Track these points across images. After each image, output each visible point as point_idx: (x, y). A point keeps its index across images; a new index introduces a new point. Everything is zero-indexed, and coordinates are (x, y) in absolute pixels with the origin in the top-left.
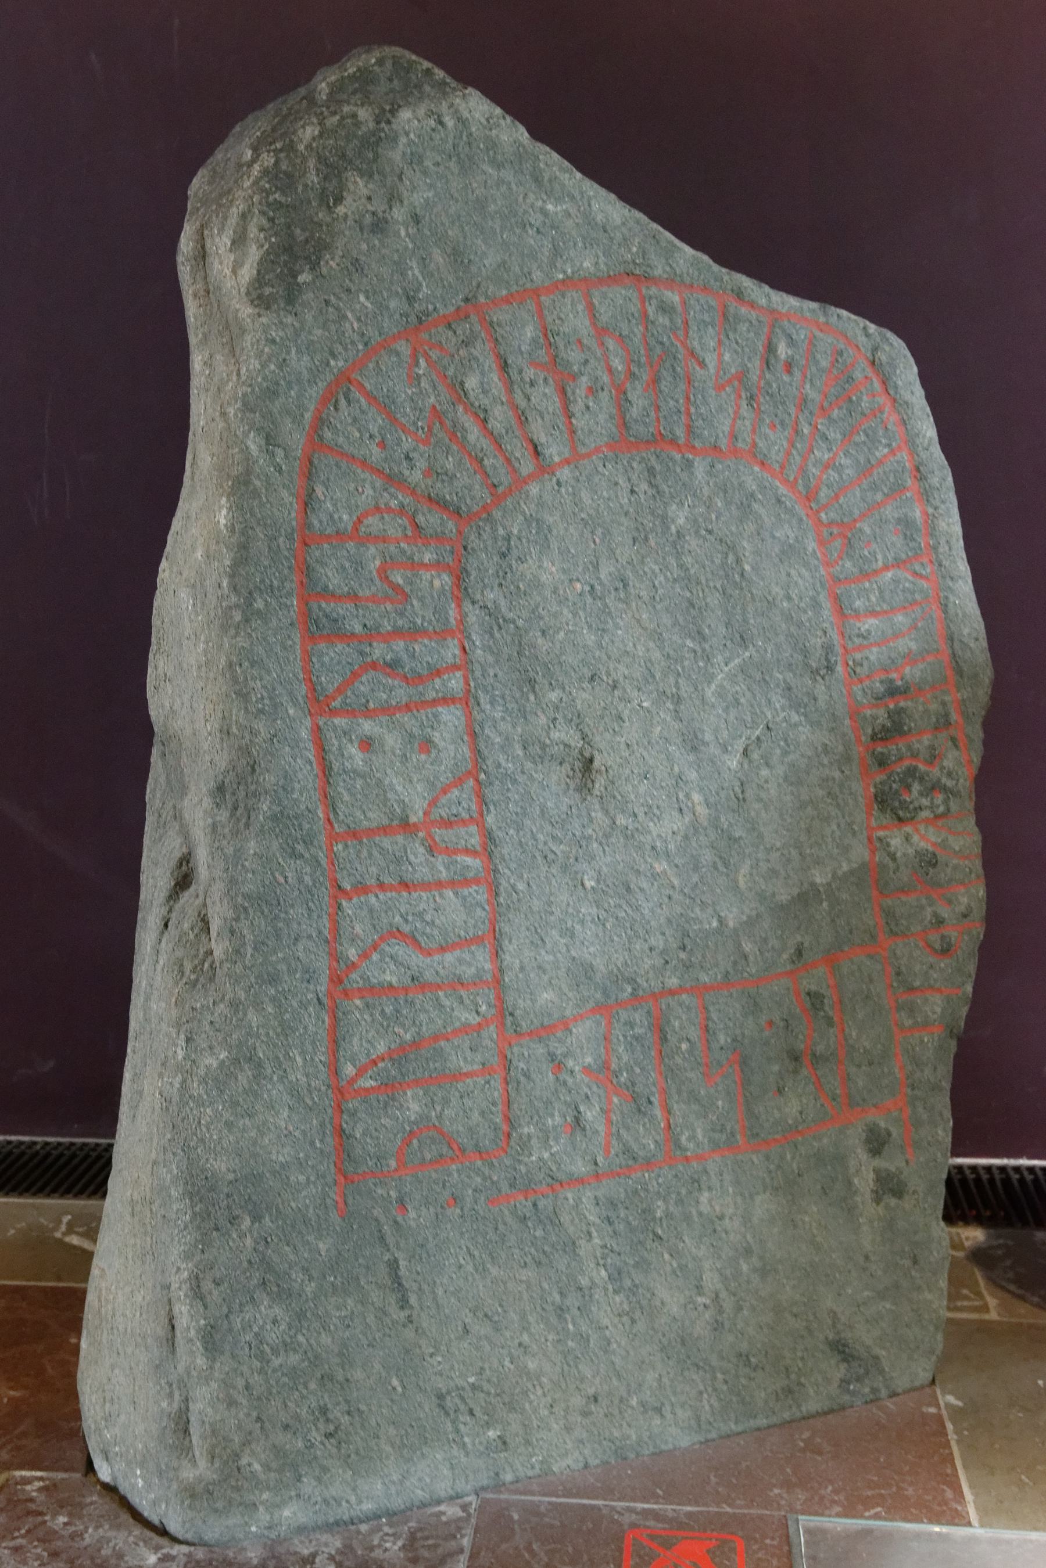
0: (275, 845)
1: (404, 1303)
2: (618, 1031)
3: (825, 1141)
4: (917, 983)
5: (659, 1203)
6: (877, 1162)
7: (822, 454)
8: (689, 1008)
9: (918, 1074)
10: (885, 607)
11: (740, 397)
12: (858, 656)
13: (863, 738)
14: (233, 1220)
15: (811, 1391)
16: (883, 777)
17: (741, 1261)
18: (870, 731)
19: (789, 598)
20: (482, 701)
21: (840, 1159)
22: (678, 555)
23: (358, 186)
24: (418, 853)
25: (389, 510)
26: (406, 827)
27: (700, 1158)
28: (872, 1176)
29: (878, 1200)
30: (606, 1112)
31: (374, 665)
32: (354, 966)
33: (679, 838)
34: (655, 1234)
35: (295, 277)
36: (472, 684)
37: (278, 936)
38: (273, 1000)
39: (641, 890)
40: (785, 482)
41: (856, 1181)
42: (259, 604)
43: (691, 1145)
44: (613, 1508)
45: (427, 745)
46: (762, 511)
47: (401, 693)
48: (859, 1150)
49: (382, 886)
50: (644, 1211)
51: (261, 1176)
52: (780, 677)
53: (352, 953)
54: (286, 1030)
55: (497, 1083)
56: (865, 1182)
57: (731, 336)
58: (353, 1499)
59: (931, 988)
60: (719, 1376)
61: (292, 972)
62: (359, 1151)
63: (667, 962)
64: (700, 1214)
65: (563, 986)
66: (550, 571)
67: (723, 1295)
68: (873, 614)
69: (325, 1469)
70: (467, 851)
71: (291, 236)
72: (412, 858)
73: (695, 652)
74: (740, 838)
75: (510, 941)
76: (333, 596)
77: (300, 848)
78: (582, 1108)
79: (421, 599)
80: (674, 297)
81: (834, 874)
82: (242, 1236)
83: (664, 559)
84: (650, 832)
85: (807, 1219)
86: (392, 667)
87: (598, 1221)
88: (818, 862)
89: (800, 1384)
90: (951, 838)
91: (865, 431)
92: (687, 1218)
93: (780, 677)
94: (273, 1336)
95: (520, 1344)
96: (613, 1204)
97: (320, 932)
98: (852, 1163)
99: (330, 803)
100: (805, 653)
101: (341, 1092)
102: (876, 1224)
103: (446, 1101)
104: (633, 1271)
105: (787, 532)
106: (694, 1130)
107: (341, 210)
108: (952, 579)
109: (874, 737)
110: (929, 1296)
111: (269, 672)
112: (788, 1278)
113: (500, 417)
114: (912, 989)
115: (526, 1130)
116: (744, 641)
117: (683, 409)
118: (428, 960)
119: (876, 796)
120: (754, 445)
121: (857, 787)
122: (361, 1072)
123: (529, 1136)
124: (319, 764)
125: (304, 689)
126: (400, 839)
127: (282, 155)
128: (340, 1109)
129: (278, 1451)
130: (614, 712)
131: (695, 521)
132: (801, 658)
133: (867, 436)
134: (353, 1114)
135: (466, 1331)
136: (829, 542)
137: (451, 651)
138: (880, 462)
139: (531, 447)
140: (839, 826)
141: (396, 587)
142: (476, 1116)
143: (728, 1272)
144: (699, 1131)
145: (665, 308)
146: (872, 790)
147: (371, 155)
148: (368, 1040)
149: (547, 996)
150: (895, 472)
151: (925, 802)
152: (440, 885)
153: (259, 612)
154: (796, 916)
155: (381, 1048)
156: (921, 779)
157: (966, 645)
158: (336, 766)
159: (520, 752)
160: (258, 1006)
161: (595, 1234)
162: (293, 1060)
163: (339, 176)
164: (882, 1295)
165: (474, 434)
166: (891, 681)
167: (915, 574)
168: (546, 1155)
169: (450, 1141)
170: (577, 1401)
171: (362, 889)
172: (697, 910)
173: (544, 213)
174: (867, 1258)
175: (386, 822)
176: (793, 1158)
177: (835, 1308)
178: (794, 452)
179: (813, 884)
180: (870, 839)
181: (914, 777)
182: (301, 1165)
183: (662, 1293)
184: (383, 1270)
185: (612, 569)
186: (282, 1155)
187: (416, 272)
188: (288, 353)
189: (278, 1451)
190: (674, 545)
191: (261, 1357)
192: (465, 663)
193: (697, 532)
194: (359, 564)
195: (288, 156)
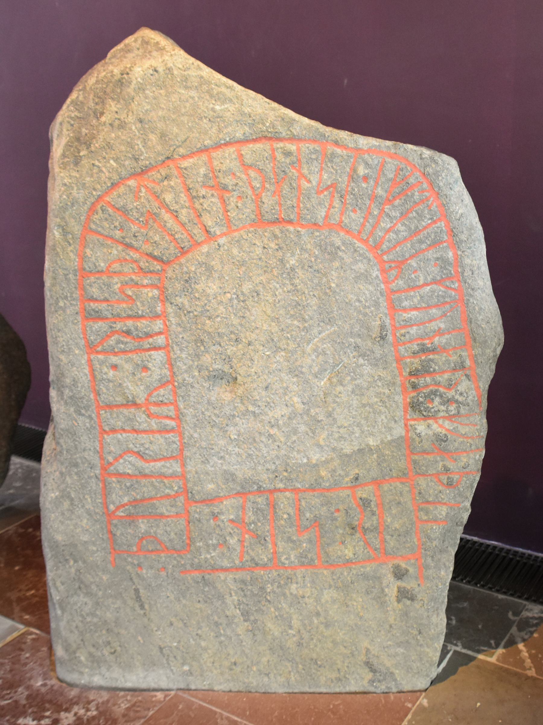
0: (72, 409)
1: (142, 607)
2: (249, 505)
3: (368, 569)
4: (431, 499)
5: (269, 586)
6: (399, 583)
7: (385, 224)
8: (288, 498)
9: (429, 544)
10: (424, 305)
11: (334, 196)
12: (403, 331)
13: (404, 374)
15: (352, 682)
16: (414, 394)
17: (314, 618)
18: (408, 370)
19: (359, 301)
20: (175, 349)
21: (379, 579)
22: (291, 279)
23: (112, 106)
24: (141, 417)
25: (126, 260)
26: (135, 404)
27: (292, 568)
28: (396, 589)
29: (399, 601)
30: (241, 542)
31: (117, 332)
32: (111, 464)
33: (286, 418)
34: (267, 599)
35: (79, 153)
36: (170, 341)
37: (76, 448)
38: (77, 474)
39: (262, 442)
40: (361, 240)
41: (386, 590)
42: (61, 304)
43: (287, 562)
44: (221, 715)
45: (145, 368)
46: (344, 256)
47: (131, 344)
48: (389, 576)
49: (124, 430)
50: (260, 588)
51: (76, 545)
52: (353, 340)
53: (111, 459)
54: (83, 487)
55: (183, 522)
56: (392, 592)
57: (329, 165)
58: (123, 680)
59: (440, 503)
60: (300, 666)
61: (83, 463)
62: (119, 541)
63: (277, 477)
64: (291, 594)
65: (219, 483)
66: (213, 287)
67: (303, 631)
68: (416, 309)
69: (110, 666)
71: (80, 132)
72: (138, 419)
73: (299, 327)
74: (322, 420)
75: (190, 460)
76: (96, 300)
77: (83, 411)
78: (228, 538)
79: (142, 302)
80: (293, 148)
81: (382, 442)
82: (70, 567)
83: (282, 281)
84: (268, 415)
85: (355, 604)
86: (128, 333)
87: (235, 589)
88: (372, 434)
89: (345, 677)
90: (459, 426)
91: (416, 211)
92: (284, 595)
93: (353, 340)
94: (87, 609)
95: (197, 634)
96: (243, 582)
97: (95, 448)
98: (385, 582)
99: (98, 394)
100: (368, 329)
101: (110, 515)
102: (397, 612)
103: (158, 526)
104: (255, 613)
105: (361, 267)
106: (289, 555)
107: (103, 119)
108: (473, 289)
109: (411, 374)
110: (427, 650)
111: (66, 334)
112: (341, 629)
113: (184, 215)
114: (428, 502)
115: (198, 544)
116: (330, 321)
117: (295, 205)
118: (147, 465)
119: (410, 404)
120: (341, 221)
121: (399, 399)
122: (118, 508)
123: (200, 547)
124: (91, 375)
125: (83, 342)
126: (133, 410)
127: (81, 93)
128: (109, 523)
129: (91, 655)
130: (248, 356)
131: (301, 262)
132: (366, 332)
133: (418, 213)
134: (116, 526)
135: (171, 624)
136: (389, 271)
137: (158, 325)
138: (425, 228)
139: (204, 228)
140: (386, 417)
141: (129, 296)
142: (172, 535)
143: (306, 622)
144: (292, 556)
145: (288, 154)
146: (408, 400)
147: (119, 91)
148: (119, 496)
149: (211, 486)
150: (436, 233)
151: (443, 408)
152: (152, 432)
153: (61, 307)
154: (356, 460)
155: (126, 500)
156: (441, 396)
157: (479, 326)
158: (99, 377)
159: (196, 374)
160: (70, 475)
161: (233, 594)
162: (86, 499)
163: (103, 102)
164: (399, 645)
165: (171, 223)
166: (424, 345)
167: (447, 287)
168: (209, 556)
169: (161, 543)
170: (226, 663)
171: (114, 431)
172: (295, 453)
173: (213, 110)
174: (391, 626)
175: (125, 402)
176: (348, 575)
177: (369, 647)
178: (367, 224)
179: (368, 445)
180: (406, 425)
181: (436, 395)
182: (94, 544)
183: (269, 625)
184: (133, 592)
185: (251, 287)
186: (85, 538)
187: (141, 146)
188: (73, 189)
189: (91, 655)
190: (289, 274)
191: (82, 616)
193: (303, 268)
194: (109, 286)
195: (83, 94)
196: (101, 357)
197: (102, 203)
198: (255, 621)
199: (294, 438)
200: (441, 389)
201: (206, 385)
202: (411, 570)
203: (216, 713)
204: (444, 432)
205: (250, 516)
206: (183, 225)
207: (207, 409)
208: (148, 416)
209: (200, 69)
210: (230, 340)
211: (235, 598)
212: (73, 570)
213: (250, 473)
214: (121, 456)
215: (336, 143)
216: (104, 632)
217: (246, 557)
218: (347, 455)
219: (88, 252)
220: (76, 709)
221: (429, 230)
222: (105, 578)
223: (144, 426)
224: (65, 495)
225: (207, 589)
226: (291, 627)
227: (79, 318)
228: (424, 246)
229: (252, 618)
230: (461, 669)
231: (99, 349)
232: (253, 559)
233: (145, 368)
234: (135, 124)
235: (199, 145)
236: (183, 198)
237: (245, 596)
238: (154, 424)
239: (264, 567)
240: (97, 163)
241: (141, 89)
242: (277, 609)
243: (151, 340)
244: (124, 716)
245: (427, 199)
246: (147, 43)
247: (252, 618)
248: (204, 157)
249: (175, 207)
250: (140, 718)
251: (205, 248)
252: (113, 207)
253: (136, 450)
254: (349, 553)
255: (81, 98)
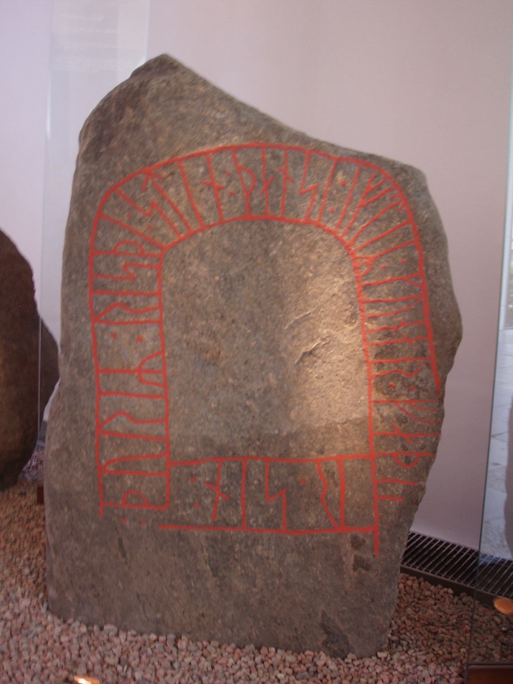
0: (76, 370)
1: (124, 555)
3: (328, 537)
6: (356, 552)
14: (62, 508)
23: (130, 112)
28: (352, 558)
29: (355, 569)
30: (215, 502)
32: (105, 422)
41: (344, 558)
48: (347, 545)
53: (105, 417)
64: (257, 554)
70: (156, 384)
78: (203, 498)
85: (315, 569)
92: (251, 555)
96: (215, 540)
115: (176, 502)
122: (108, 463)
135: (149, 573)
137: (154, 301)
152: (143, 396)
155: (116, 456)
171: (109, 392)
174: (346, 593)
176: (309, 542)
183: (236, 582)
192: (160, 306)
196: (103, 326)
198: (224, 577)
199: (268, 410)
202: (368, 542)
204: (404, 414)
205: (224, 480)
210: (216, 318)
211: (206, 554)
212: (67, 517)
213: (225, 440)
214: (114, 416)
216: (90, 576)
217: (218, 518)
219: (100, 233)
222: (93, 526)
224: (64, 448)
225: (181, 544)
226: (255, 586)
227: (88, 290)
229: (221, 574)
232: (224, 520)
239: (234, 526)
242: (243, 567)
245: (398, 204)
247: (221, 574)
253: (127, 411)
254: (311, 520)
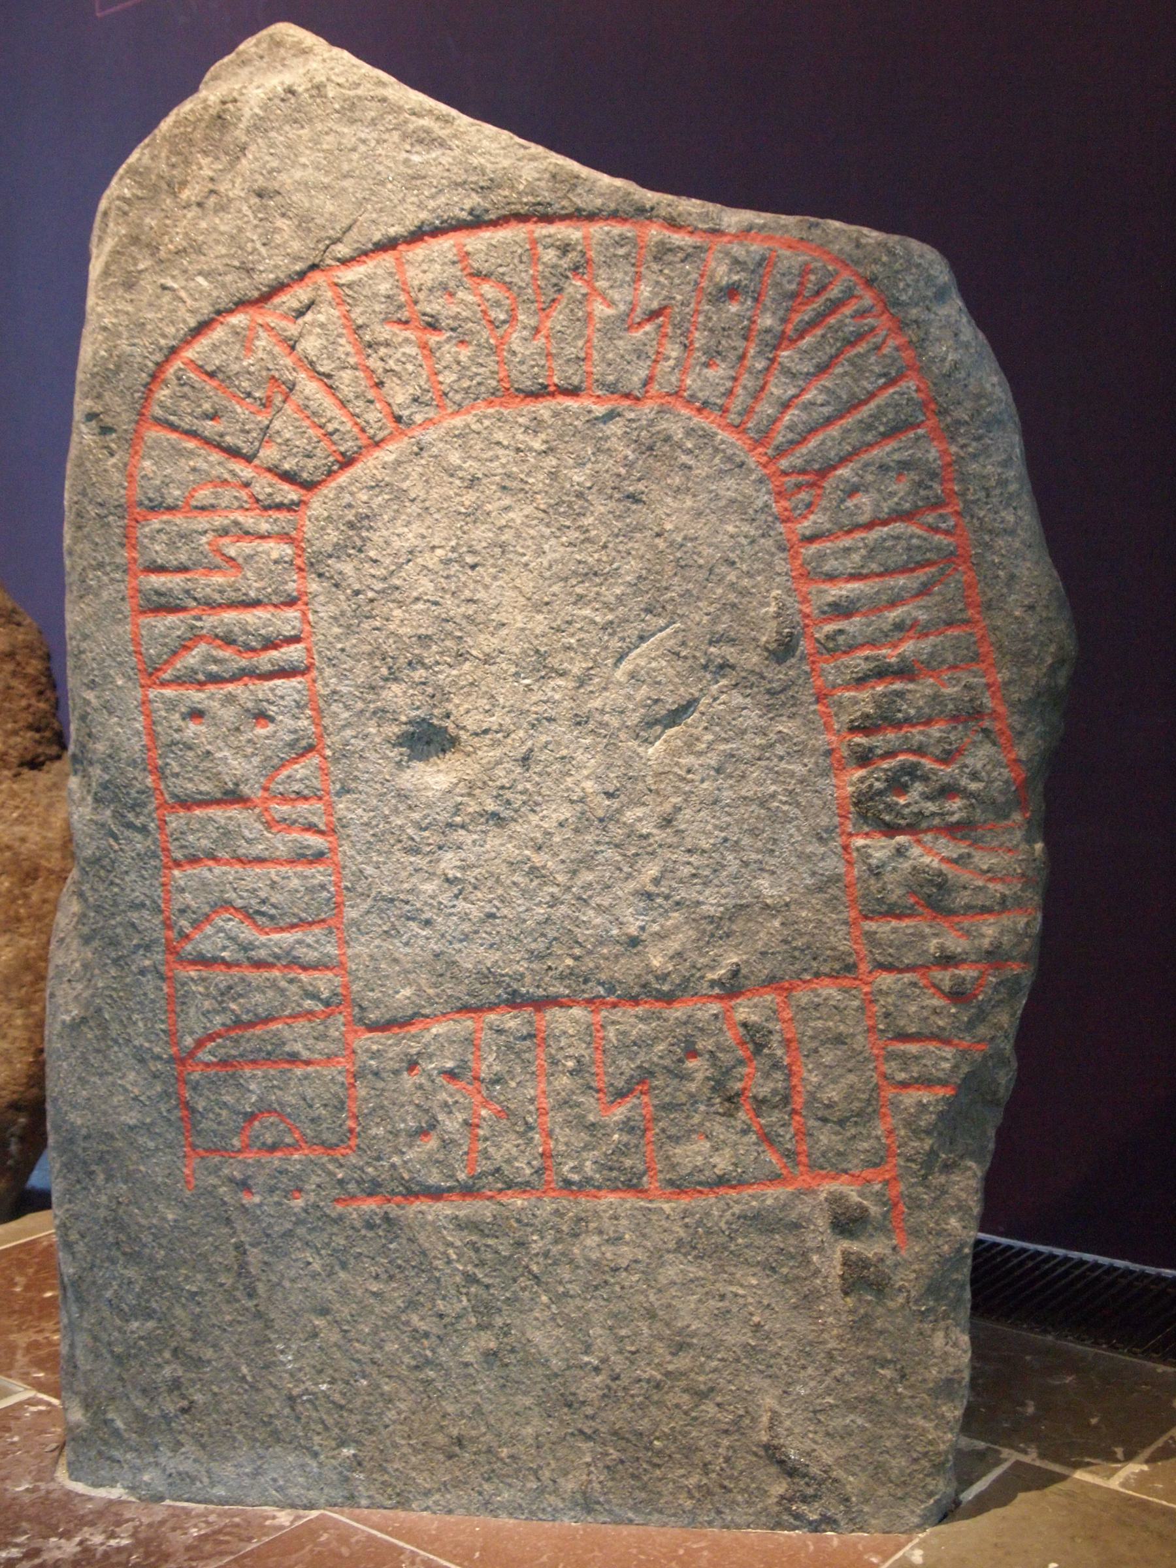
7: (778, 389)
23: (206, 166)
28: (838, 1255)
35: (135, 265)
72: (246, 833)
76: (162, 569)
107: (185, 195)
122: (200, 1044)
171: (194, 860)
177: (777, 1408)
182: (148, 1128)
196: (168, 692)
197: (178, 364)
198: (506, 1330)
200: (927, 764)
201: (394, 753)
203: (401, 1551)
206: (343, 404)
207: (396, 811)
208: (268, 825)
209: (383, 84)
214: (207, 918)
215: (673, 223)
218: (711, 919)
220: (86, 1532)
221: (879, 401)
223: (258, 849)
228: (869, 437)
230: (1021, 1496)
231: (166, 676)
233: (262, 716)
234: (246, 200)
235: (377, 236)
236: (345, 346)
237: (482, 1264)
238: (281, 843)
240: (170, 283)
241: (259, 126)
243: (274, 654)
244: (188, 1548)
246: (279, 44)
247: (499, 1321)
248: (387, 260)
249: (325, 367)
250: (222, 1554)
251: (387, 454)
252: (200, 369)
253: (239, 903)
255: (146, 160)
